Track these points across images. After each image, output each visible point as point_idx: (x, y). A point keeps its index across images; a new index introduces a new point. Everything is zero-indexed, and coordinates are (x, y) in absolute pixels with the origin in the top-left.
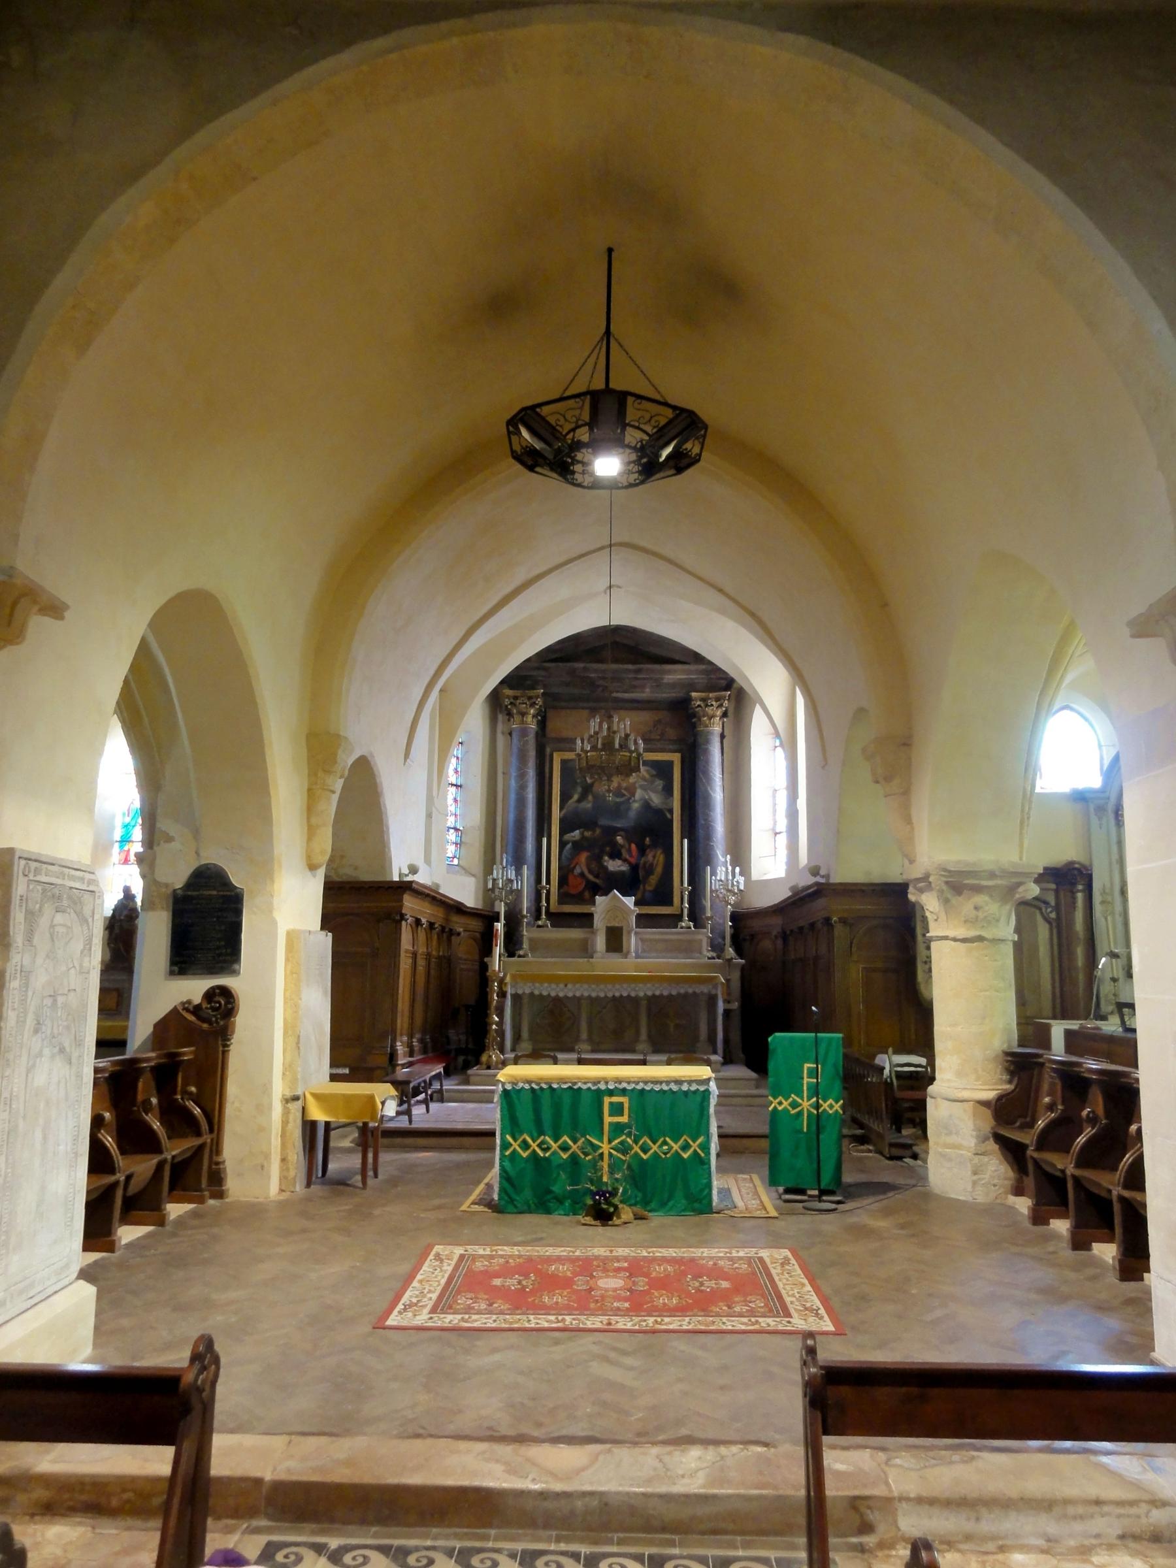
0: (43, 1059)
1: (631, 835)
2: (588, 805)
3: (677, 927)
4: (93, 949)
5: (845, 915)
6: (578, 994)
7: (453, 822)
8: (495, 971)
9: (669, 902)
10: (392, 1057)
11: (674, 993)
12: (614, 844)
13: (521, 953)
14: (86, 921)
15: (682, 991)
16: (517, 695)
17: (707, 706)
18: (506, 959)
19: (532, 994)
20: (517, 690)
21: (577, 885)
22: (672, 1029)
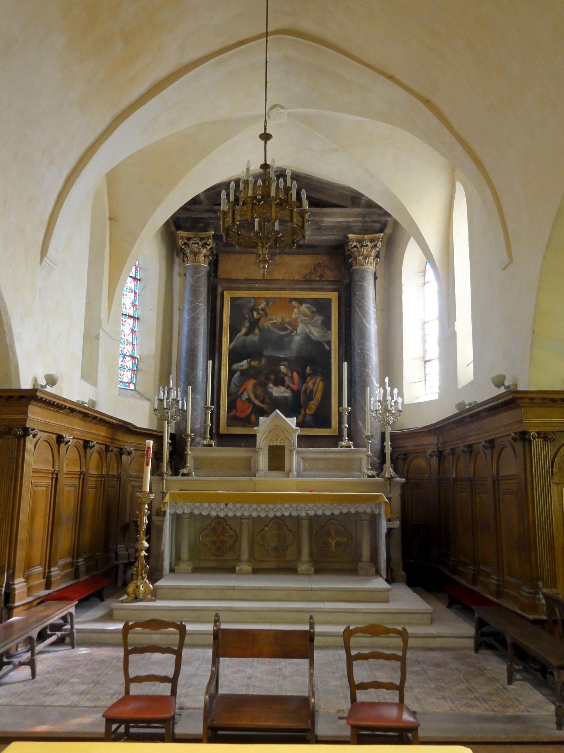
1: (293, 363)
2: (254, 338)
3: (337, 447)
5: (542, 429)
6: (239, 514)
7: (130, 351)
8: (145, 492)
9: (327, 424)
10: (9, 596)
11: (337, 512)
12: (277, 372)
13: (185, 471)
15: (345, 511)
16: (190, 236)
17: (362, 246)
18: (170, 478)
19: (191, 514)
20: (191, 231)
21: (245, 410)
22: (333, 548)
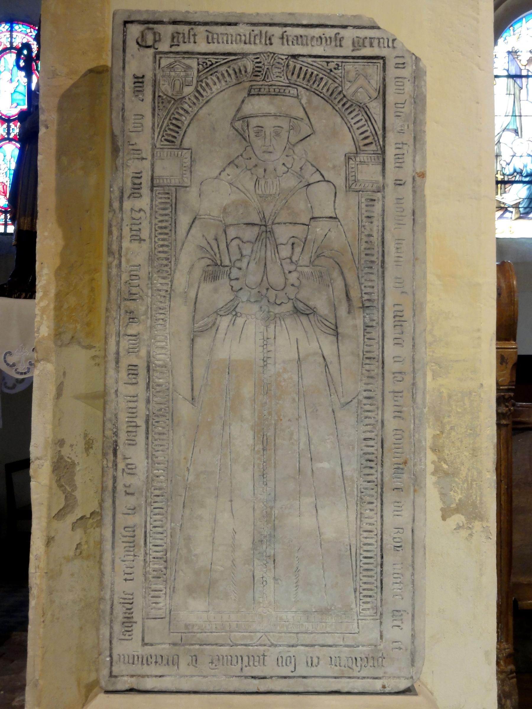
0: (240, 321)
4: (391, 151)
14: (364, 108)
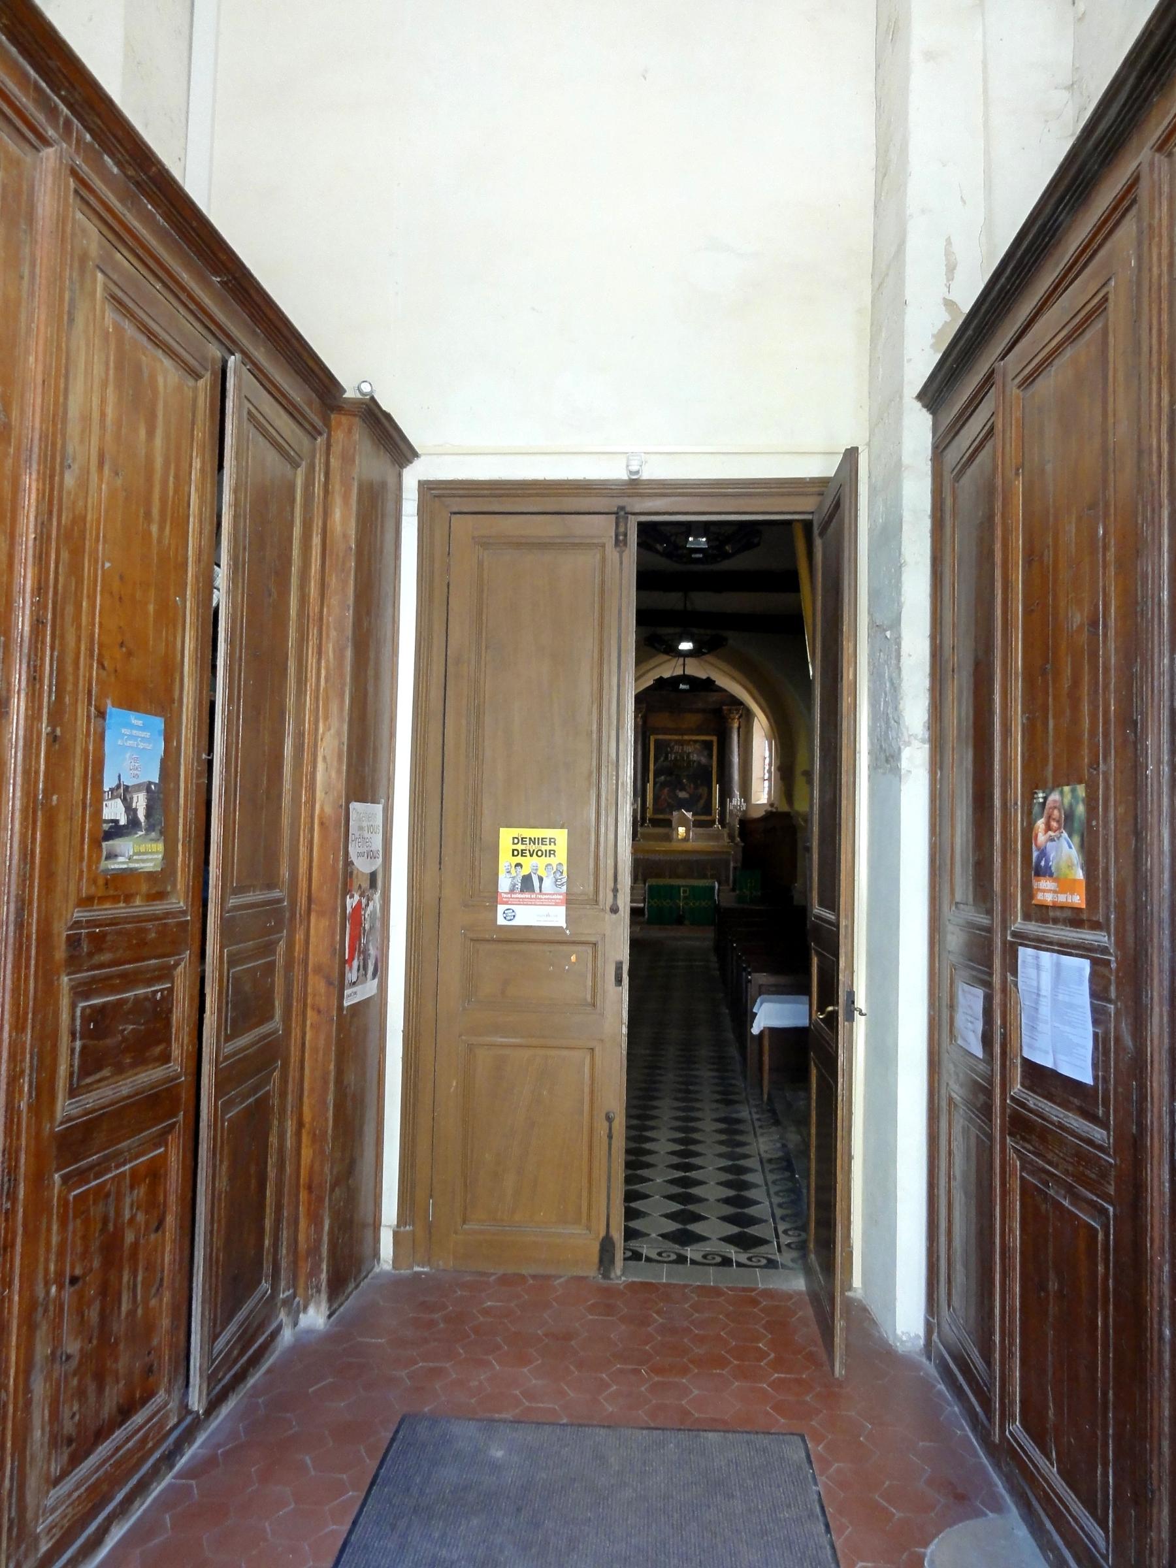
9: (710, 814)
